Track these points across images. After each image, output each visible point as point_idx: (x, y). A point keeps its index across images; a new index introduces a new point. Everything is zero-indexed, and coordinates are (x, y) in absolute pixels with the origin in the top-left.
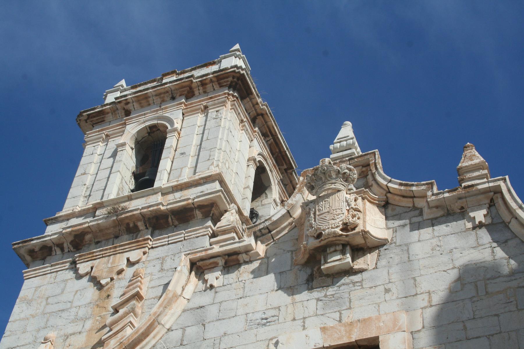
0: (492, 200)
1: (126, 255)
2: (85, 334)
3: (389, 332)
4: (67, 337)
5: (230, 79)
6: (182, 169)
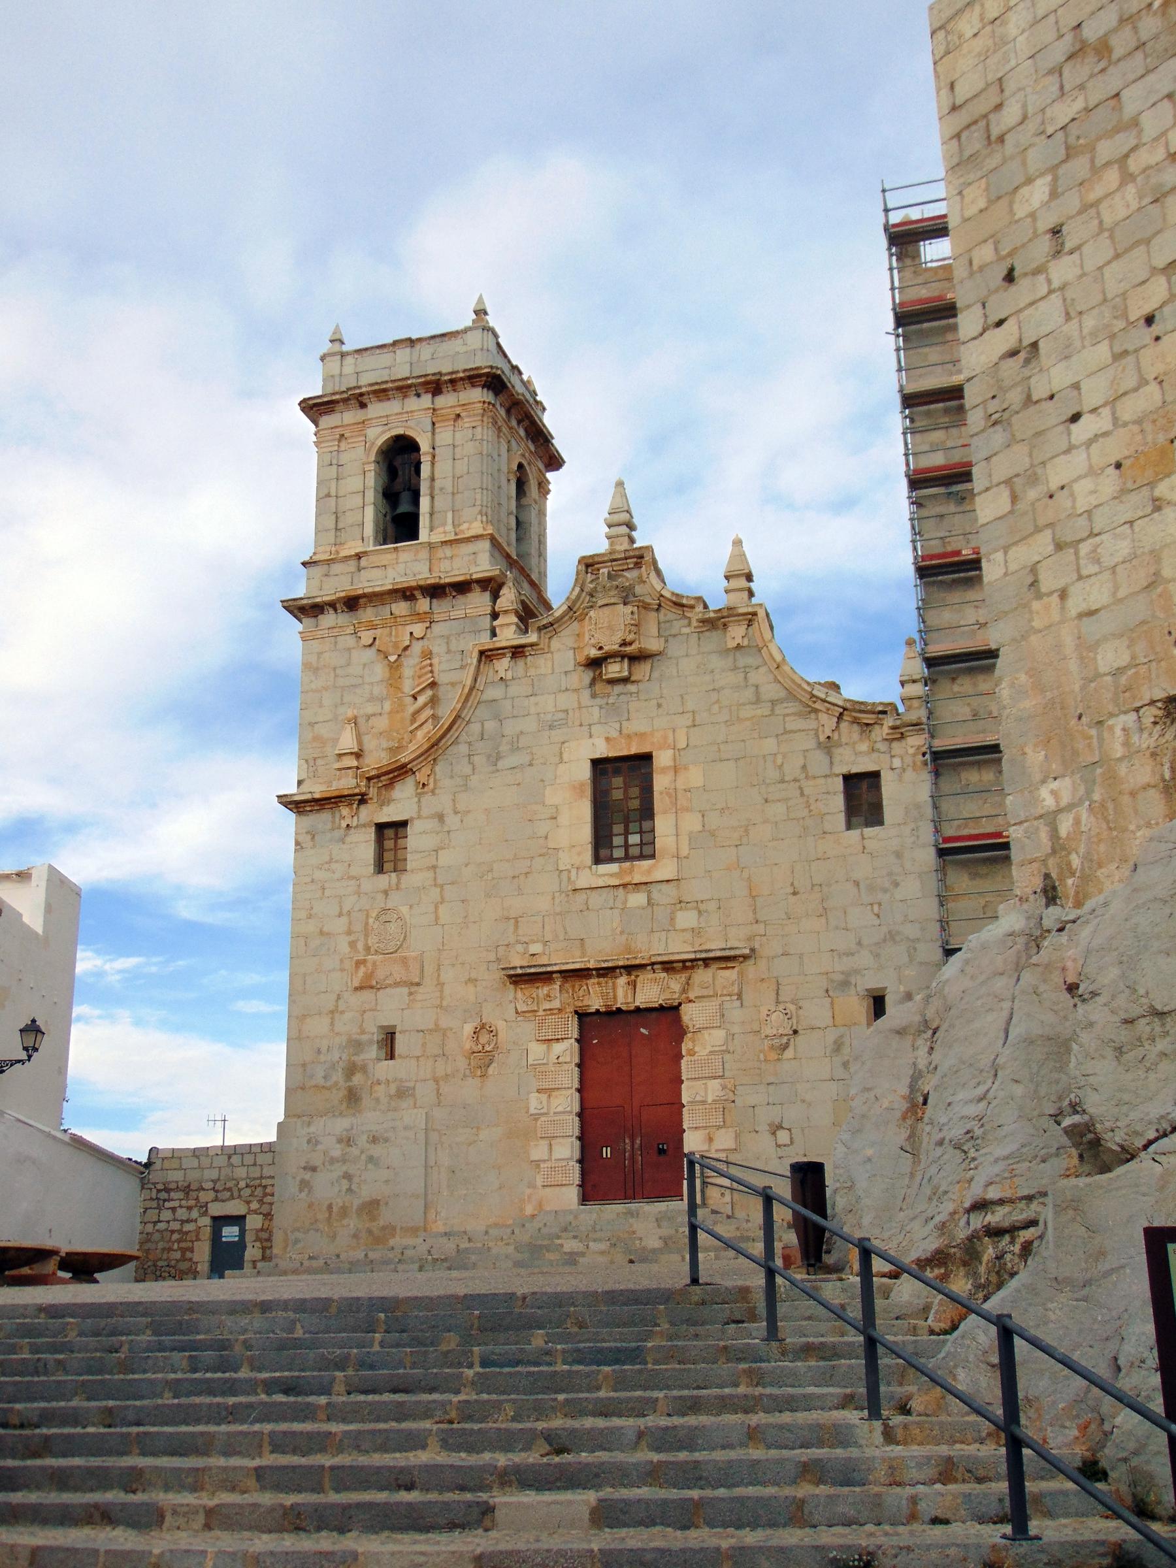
0: (750, 620)
1: (409, 628)
2: (386, 716)
3: (660, 748)
4: (368, 717)
5: (484, 379)
6: (446, 512)
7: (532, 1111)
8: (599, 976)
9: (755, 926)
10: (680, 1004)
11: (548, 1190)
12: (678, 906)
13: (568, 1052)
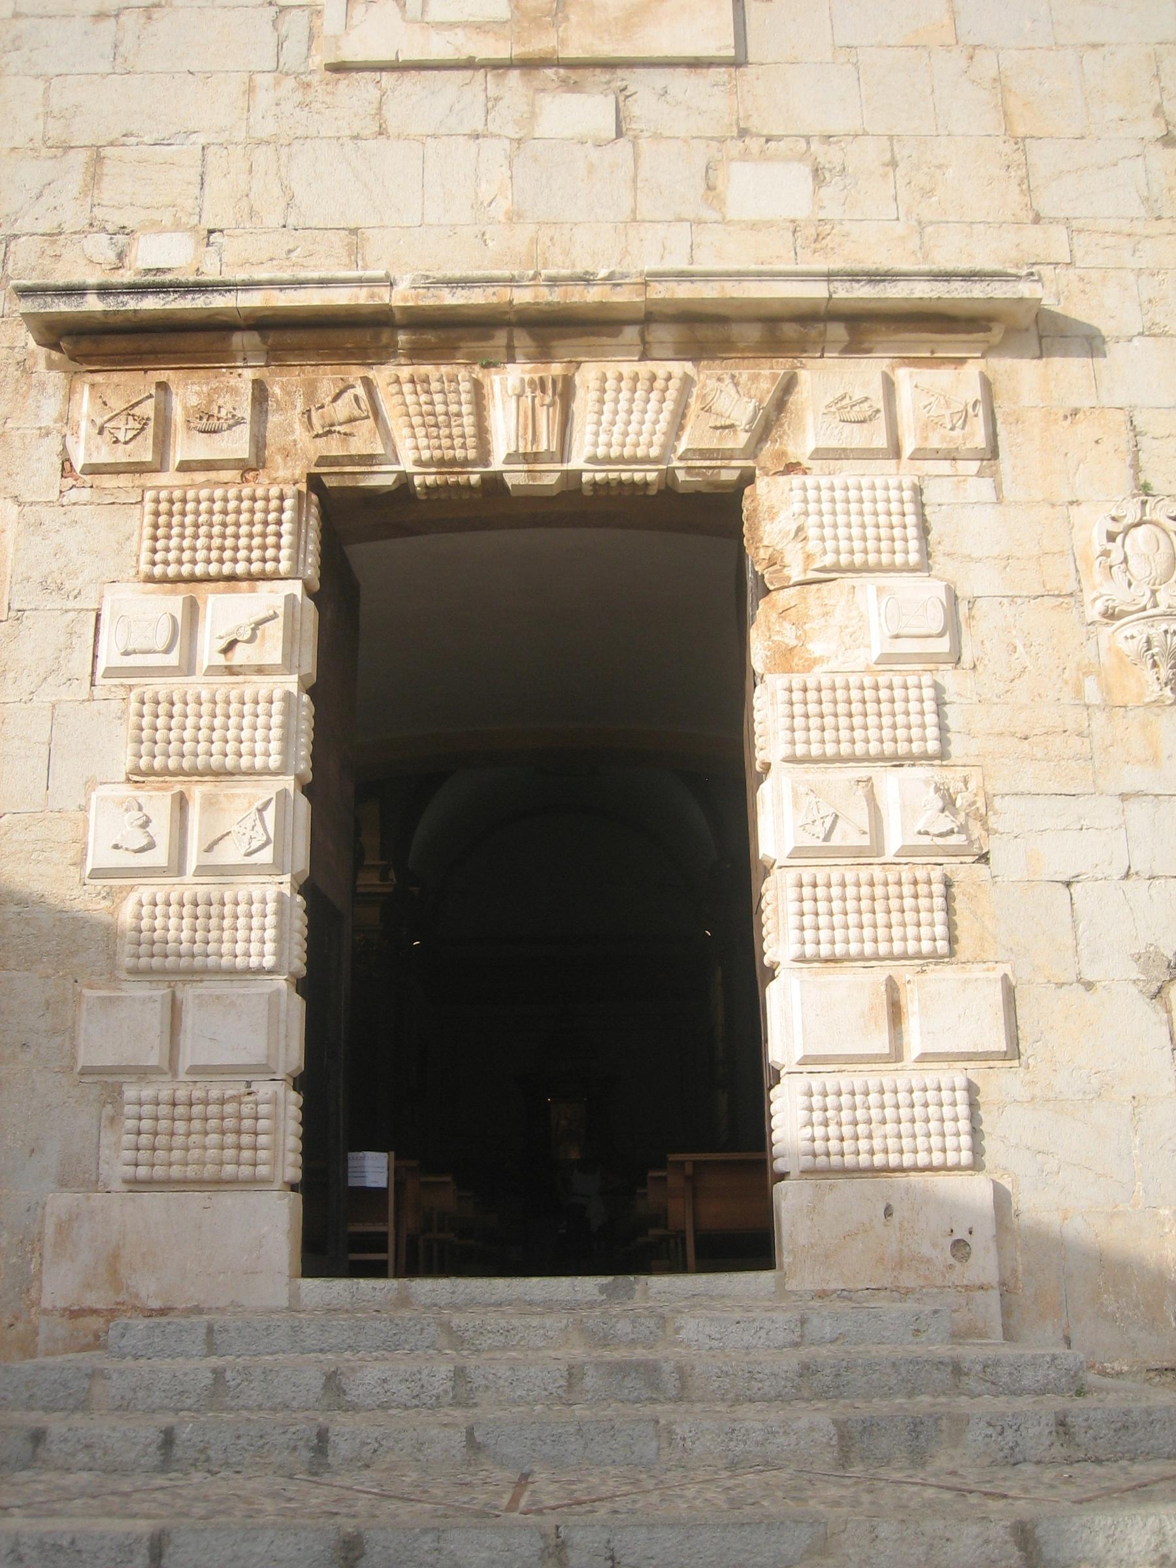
7: (99, 856)
8: (417, 354)
9: (1034, 232)
10: (748, 478)
11: (152, 1200)
12: (735, 147)
13: (275, 632)
